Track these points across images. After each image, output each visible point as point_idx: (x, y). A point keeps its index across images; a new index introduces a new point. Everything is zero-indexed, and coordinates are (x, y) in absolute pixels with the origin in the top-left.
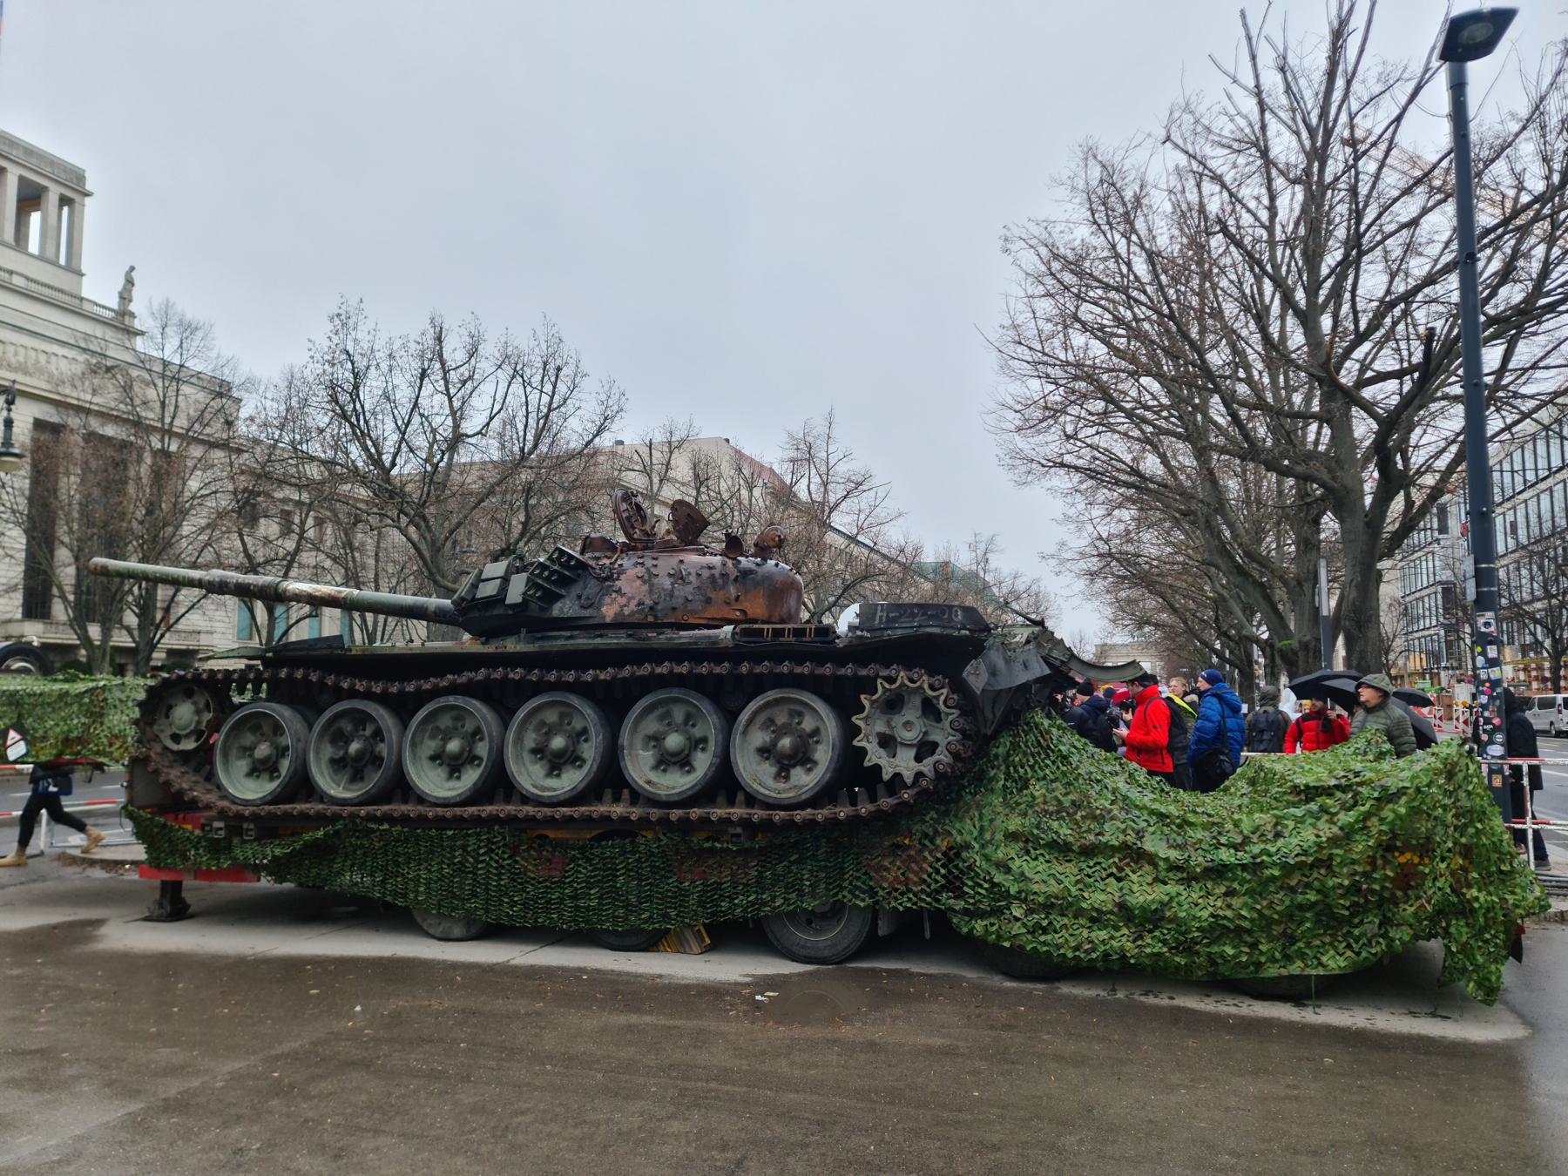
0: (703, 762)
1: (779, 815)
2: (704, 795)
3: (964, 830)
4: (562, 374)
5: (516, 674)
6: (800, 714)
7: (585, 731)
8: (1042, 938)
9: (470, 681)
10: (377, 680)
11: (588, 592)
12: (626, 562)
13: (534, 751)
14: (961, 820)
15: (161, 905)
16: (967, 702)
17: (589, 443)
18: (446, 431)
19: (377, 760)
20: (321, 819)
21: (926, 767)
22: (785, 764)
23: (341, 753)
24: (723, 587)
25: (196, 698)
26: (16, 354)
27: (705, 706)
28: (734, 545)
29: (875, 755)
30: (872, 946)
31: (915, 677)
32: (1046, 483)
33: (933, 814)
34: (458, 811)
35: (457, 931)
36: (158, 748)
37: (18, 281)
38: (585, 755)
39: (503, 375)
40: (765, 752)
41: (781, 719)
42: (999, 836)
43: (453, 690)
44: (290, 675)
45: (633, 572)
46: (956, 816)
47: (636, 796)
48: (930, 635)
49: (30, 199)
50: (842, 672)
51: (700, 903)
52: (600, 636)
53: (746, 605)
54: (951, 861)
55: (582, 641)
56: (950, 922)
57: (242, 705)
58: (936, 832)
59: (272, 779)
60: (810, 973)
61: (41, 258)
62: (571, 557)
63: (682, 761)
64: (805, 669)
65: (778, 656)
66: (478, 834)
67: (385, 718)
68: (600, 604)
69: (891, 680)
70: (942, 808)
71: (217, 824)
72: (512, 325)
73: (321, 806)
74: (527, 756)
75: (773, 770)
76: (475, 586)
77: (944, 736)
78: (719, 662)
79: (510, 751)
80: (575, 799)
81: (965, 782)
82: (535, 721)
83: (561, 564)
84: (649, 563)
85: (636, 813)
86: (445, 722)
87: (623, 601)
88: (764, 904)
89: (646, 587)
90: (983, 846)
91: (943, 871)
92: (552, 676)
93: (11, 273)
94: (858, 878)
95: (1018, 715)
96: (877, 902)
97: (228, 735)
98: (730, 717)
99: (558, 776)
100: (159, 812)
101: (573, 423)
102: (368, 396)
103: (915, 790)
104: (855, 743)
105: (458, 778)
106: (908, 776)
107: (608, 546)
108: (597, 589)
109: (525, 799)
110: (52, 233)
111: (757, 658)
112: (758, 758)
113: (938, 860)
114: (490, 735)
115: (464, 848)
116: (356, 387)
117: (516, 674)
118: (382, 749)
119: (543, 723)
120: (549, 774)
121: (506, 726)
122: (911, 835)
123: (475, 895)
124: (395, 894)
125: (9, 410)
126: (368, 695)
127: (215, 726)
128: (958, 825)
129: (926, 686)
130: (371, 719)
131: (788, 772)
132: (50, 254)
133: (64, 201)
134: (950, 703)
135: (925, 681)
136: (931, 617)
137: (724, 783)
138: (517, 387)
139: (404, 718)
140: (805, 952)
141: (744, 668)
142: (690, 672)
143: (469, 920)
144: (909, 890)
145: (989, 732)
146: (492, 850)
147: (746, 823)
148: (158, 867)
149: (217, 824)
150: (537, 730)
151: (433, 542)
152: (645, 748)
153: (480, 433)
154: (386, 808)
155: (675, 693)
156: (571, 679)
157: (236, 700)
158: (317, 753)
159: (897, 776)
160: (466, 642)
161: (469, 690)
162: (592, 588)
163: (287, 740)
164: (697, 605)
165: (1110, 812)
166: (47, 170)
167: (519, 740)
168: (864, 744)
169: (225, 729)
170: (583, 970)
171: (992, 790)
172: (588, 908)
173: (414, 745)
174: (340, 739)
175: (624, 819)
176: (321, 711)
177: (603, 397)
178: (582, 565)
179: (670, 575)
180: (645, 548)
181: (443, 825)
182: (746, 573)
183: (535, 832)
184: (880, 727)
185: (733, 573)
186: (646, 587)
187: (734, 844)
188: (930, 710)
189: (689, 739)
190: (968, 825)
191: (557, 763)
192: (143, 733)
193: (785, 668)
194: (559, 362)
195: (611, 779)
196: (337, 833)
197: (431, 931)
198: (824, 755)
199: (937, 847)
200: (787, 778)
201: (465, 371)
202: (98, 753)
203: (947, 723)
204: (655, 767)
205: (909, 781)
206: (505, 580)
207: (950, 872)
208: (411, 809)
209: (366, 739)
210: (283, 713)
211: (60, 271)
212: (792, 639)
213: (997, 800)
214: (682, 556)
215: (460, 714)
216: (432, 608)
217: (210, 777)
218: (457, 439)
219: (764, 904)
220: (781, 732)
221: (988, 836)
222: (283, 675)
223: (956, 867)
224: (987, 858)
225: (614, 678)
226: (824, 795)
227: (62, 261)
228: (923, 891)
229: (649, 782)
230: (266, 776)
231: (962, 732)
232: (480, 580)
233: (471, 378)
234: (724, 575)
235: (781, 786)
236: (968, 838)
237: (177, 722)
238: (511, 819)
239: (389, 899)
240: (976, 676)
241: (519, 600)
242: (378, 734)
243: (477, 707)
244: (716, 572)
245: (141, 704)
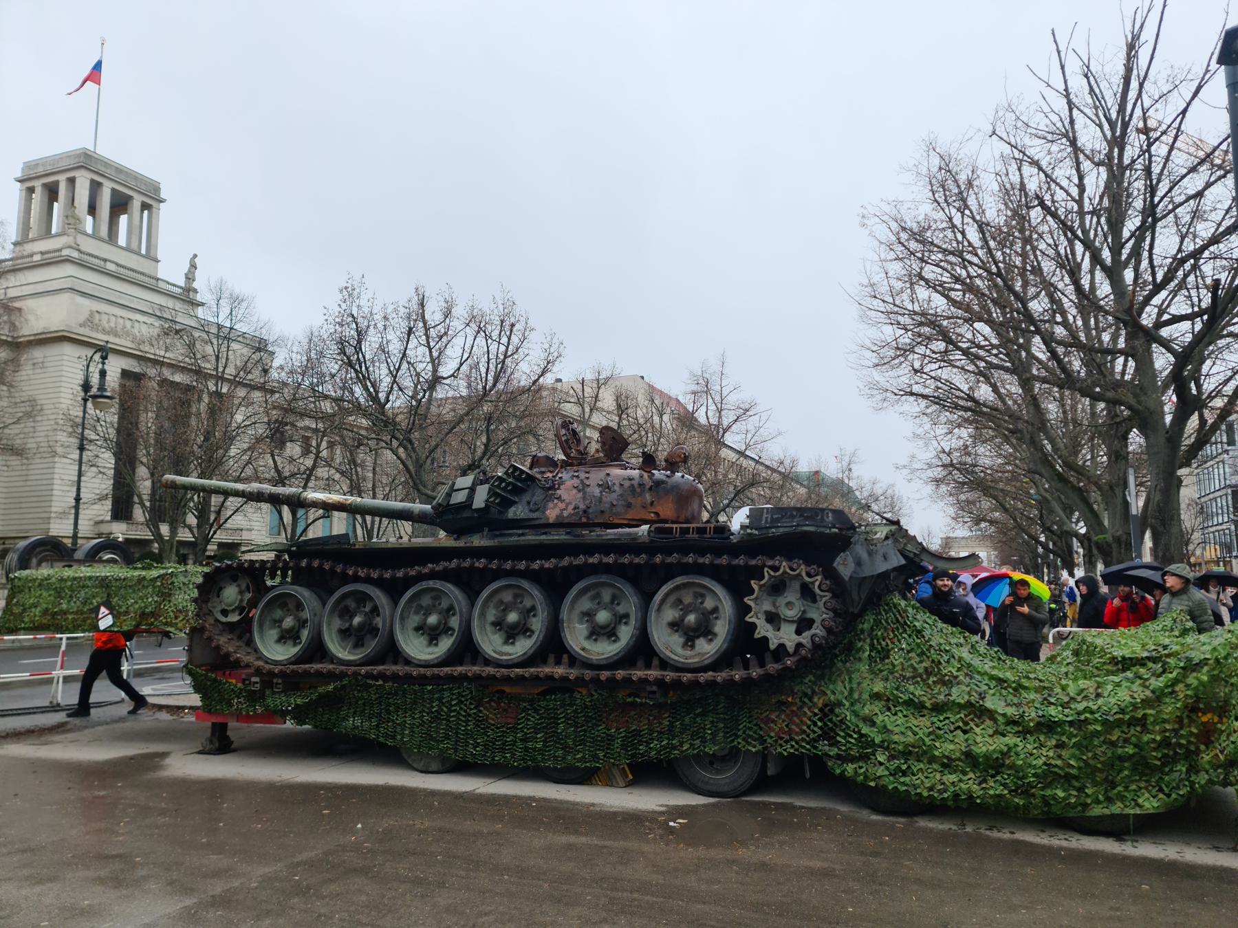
0: (626, 634)
1: (686, 677)
2: (627, 659)
3: (837, 690)
4: (515, 329)
5: (480, 563)
6: (703, 596)
7: (533, 608)
8: (902, 780)
9: (446, 569)
10: (375, 568)
11: (536, 498)
12: (565, 475)
13: (495, 624)
14: (834, 682)
15: (211, 742)
16: (838, 587)
17: (535, 382)
18: (427, 375)
19: (374, 631)
20: (331, 676)
21: (805, 639)
22: (691, 636)
23: (347, 625)
24: (640, 495)
25: (240, 582)
26: (109, 321)
27: (628, 589)
28: (649, 461)
29: (764, 629)
30: (762, 784)
31: (795, 566)
32: (898, 408)
33: (811, 677)
34: (436, 670)
35: (434, 767)
36: (212, 621)
38: (534, 628)
39: (470, 331)
40: (675, 626)
41: (688, 599)
42: (866, 696)
43: (433, 576)
44: (309, 564)
45: (570, 483)
46: (830, 679)
47: (574, 660)
48: (806, 532)
50: (736, 562)
51: (623, 747)
52: (545, 533)
53: (659, 509)
54: (826, 715)
55: (531, 538)
56: (825, 764)
57: (273, 587)
58: (814, 692)
59: (295, 645)
60: (713, 805)
62: (522, 472)
63: (610, 633)
64: (706, 560)
65: (685, 549)
66: (451, 689)
67: (380, 598)
68: (545, 509)
69: (776, 569)
70: (819, 672)
71: (254, 679)
72: (476, 292)
73: (331, 666)
74: (489, 628)
75: (682, 640)
76: (449, 495)
77: (819, 614)
78: (638, 554)
79: (475, 624)
80: (526, 662)
81: (837, 652)
82: (495, 600)
83: (514, 478)
84: (583, 476)
85: (573, 673)
86: (426, 601)
87: (562, 506)
88: (675, 748)
89: (580, 495)
90: (852, 704)
91: (820, 724)
92: (508, 565)
93: (105, 260)
94: (750, 729)
95: (879, 597)
96: (765, 748)
97: (262, 611)
98: (647, 598)
99: (513, 643)
100: (210, 670)
101: (524, 366)
102: (368, 349)
103: (796, 658)
104: (747, 619)
105: (436, 645)
106: (790, 647)
107: (551, 463)
108: (542, 497)
109: (487, 662)
110: (136, 231)
111: (668, 551)
112: (669, 631)
113: (816, 715)
114: (461, 611)
115: (440, 699)
116: (359, 342)
117: (480, 563)
118: (379, 622)
119: (501, 602)
120: (506, 642)
121: (472, 604)
122: (793, 694)
123: (447, 737)
124: (386, 736)
125: (103, 364)
126: (368, 580)
127: (253, 604)
128: (831, 687)
129: (804, 574)
130: (371, 599)
131: (693, 641)
132: (134, 246)
133: (145, 206)
134: (824, 587)
135: (803, 570)
136: (807, 518)
137: (642, 650)
138: (481, 340)
139: (395, 598)
140: (709, 787)
141: (658, 559)
142: (616, 562)
144: (792, 739)
145: (856, 611)
146: (462, 702)
147: (660, 682)
148: (210, 712)
149: (254, 679)
150: (496, 607)
151: (417, 460)
152: (581, 622)
153: (453, 375)
154: (381, 668)
156: (522, 567)
157: (269, 583)
158: (329, 625)
159: (782, 646)
160: (442, 538)
161: (444, 576)
162: (538, 496)
163: (306, 614)
164: (620, 509)
165: (956, 677)
166: (132, 184)
167: (483, 615)
168: (753, 620)
169: (261, 605)
170: (532, 799)
171: (860, 659)
172: (534, 749)
173: (402, 618)
174: (346, 614)
175: (564, 679)
176: (332, 593)
177: (547, 346)
178: (531, 478)
179: (599, 485)
180: (580, 464)
181: (424, 681)
182: (658, 484)
183: (495, 688)
184: (767, 606)
185: (649, 483)
186: (580, 495)
187: (651, 699)
188: (807, 592)
189: (615, 615)
190: (840, 686)
191: (512, 633)
192: (201, 609)
193: (690, 559)
194: (512, 320)
195: (553, 646)
196: (343, 687)
197: (415, 765)
198: (722, 628)
199: (815, 705)
200: (693, 647)
201: (441, 329)
202: (166, 624)
203: (821, 604)
204: (588, 637)
205: (791, 649)
206: (472, 490)
207: (825, 725)
208: (399, 669)
209: (366, 614)
210: (303, 593)
212: (696, 536)
213: (864, 667)
214: (609, 470)
215: (437, 594)
216: (416, 512)
217: (250, 642)
218: (436, 380)
219: (675, 748)
220: (687, 610)
221: (856, 696)
222: (304, 564)
223: (831, 720)
224: (856, 714)
225: (556, 567)
226: (722, 661)
227: (143, 252)
228: (803, 740)
229: (583, 649)
230: (290, 642)
231: (834, 611)
232: (453, 490)
233: (446, 333)
234: (641, 485)
235: (689, 653)
236: (840, 697)
237: (226, 600)
238: (478, 678)
239: (381, 739)
240: (845, 566)
241: (483, 505)
242: (375, 611)
243: (450, 589)
244: (635, 483)
245: (199, 587)
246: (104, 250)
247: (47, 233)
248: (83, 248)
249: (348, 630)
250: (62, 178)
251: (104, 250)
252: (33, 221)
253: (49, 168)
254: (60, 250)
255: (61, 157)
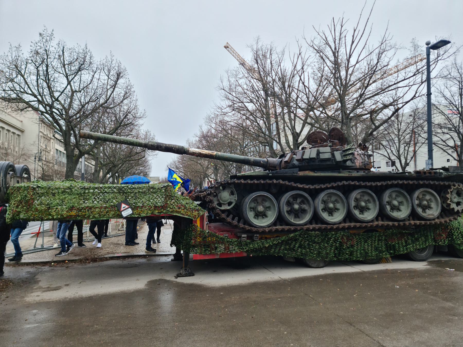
35: (321, 265)
38: (370, 207)
43: (333, 188)
143: (325, 262)
155: (397, 189)
159: (458, 211)
197: (313, 265)
216: (252, 160)
249: (290, 211)
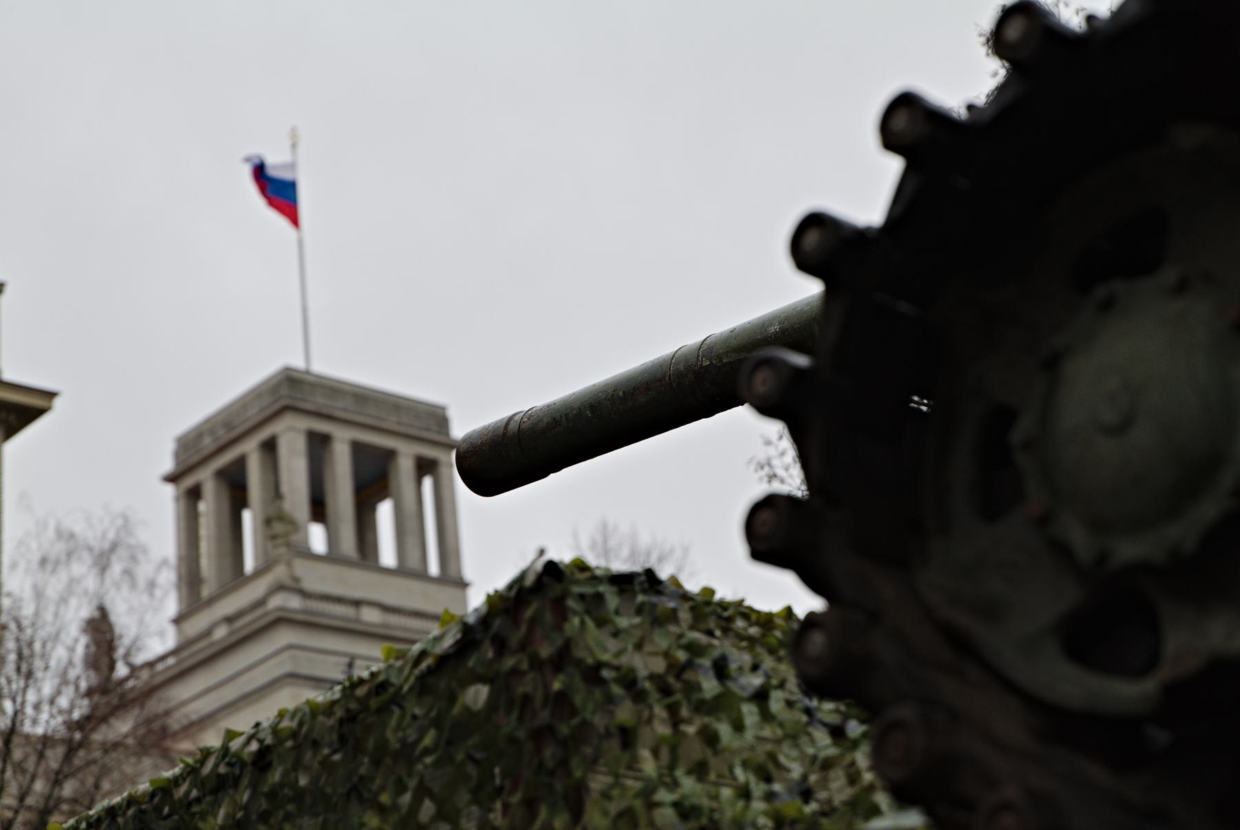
37: (370, 616)
49: (373, 481)
61: (402, 571)
93: (357, 603)
132: (413, 562)
166: (391, 423)
211: (433, 589)
227: (434, 569)
246: (355, 583)
247: (236, 576)
248: (309, 584)
250: (250, 448)
251: (355, 583)
252: (207, 564)
253: (224, 436)
254: (261, 603)
255: (243, 403)
